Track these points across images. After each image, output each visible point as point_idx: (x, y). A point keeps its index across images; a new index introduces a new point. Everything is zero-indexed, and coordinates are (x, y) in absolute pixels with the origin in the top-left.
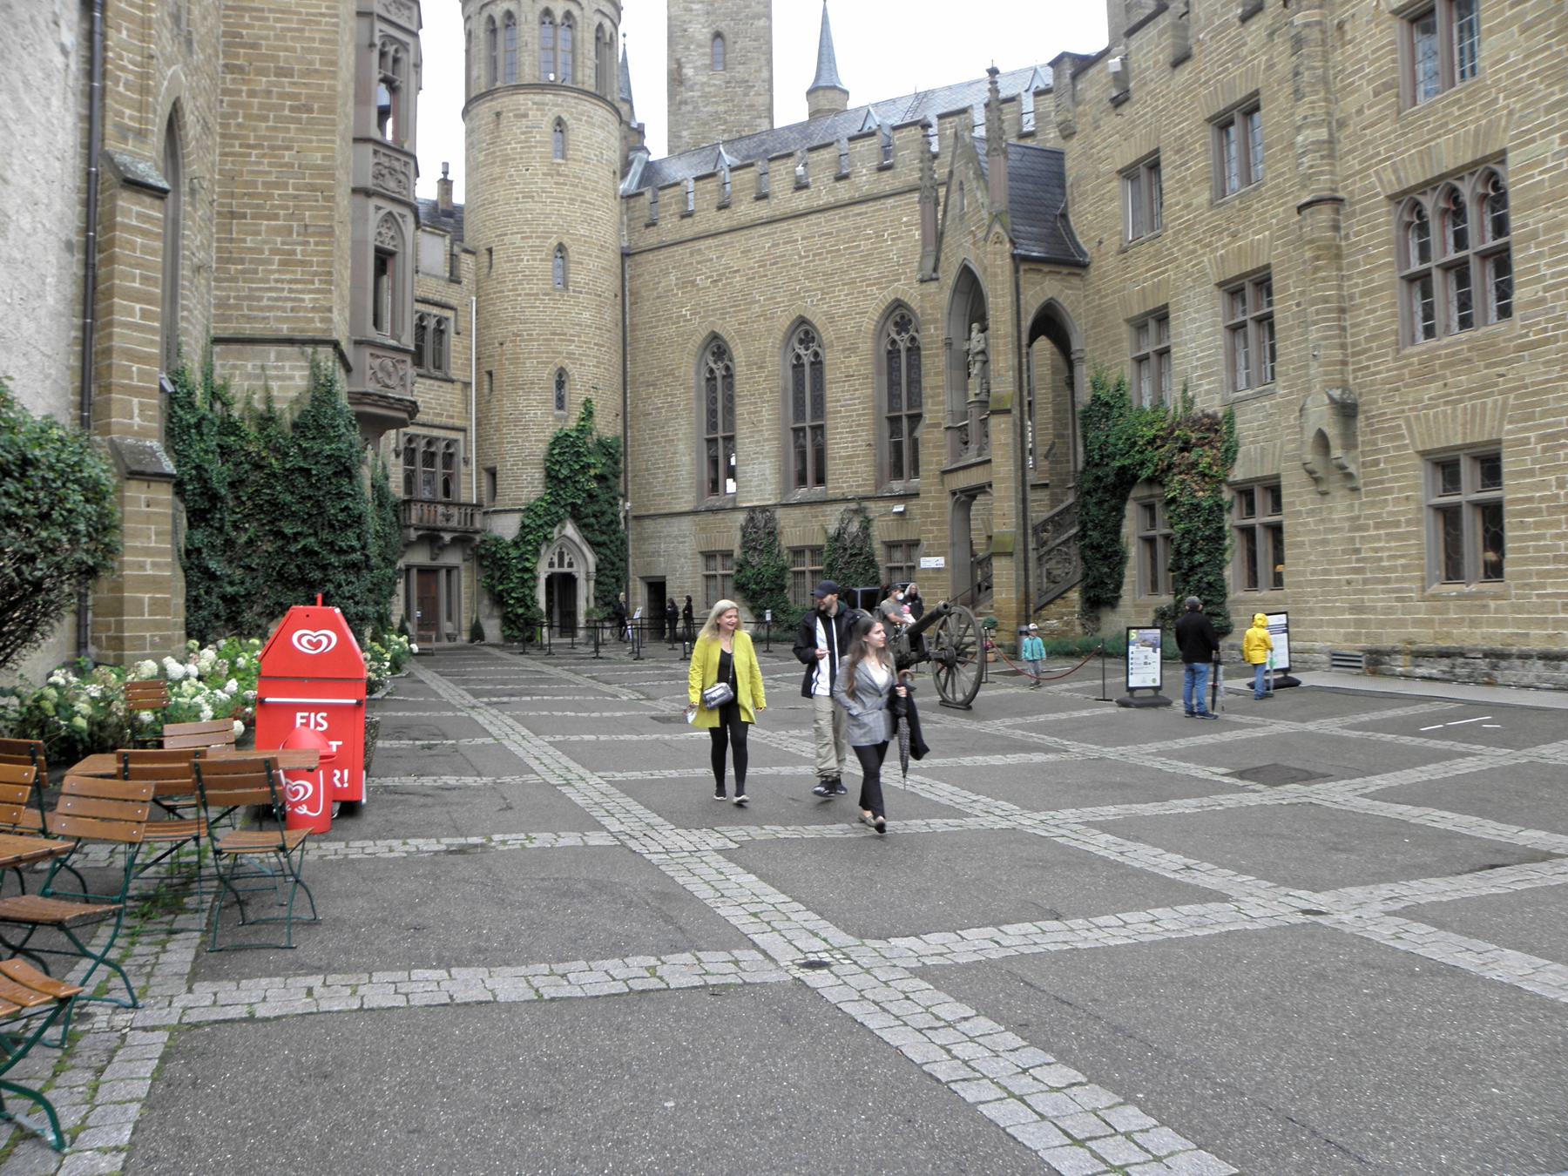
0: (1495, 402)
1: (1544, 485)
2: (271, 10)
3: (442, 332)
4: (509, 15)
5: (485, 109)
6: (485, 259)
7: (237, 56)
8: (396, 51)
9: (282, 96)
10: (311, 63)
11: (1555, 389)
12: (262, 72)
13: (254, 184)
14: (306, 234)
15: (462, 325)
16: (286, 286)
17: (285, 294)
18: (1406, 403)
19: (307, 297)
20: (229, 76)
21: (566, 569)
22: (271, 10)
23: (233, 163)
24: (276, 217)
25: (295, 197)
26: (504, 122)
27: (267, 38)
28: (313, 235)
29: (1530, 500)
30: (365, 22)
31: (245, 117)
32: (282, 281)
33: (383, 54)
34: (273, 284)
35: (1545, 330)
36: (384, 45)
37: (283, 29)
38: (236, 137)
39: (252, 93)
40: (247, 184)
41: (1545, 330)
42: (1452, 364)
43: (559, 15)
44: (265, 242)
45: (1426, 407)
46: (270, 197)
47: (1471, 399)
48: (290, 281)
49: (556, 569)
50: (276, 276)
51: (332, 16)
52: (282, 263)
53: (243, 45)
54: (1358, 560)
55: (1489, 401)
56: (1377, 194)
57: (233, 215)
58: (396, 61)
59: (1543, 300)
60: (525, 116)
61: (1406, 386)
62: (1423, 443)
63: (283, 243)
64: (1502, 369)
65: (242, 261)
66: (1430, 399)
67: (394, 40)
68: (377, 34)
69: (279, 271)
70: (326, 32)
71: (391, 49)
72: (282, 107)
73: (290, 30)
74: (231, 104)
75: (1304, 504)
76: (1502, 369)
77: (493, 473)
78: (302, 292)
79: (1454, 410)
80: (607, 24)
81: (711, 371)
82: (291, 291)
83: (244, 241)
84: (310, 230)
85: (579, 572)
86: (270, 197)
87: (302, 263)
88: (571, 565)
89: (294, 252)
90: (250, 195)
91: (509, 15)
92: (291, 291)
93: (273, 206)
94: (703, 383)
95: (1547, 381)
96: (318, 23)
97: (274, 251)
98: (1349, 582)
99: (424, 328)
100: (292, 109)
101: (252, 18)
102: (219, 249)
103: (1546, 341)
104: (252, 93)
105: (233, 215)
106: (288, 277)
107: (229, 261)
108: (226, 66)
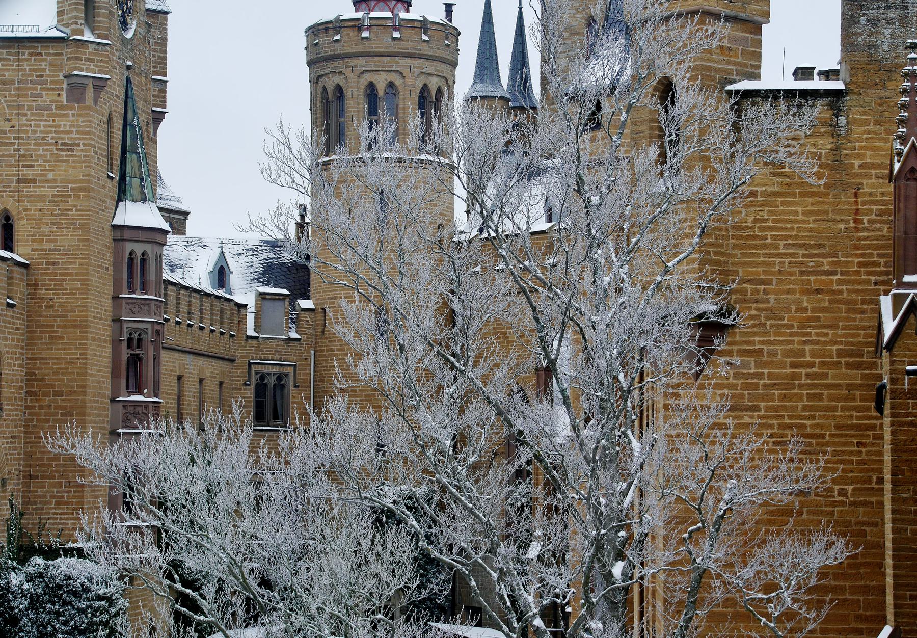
2: (50, 358)
3: (283, 386)
6: (320, 317)
7: (33, 386)
8: (140, 335)
9: (56, 408)
10: (72, 387)
12: (46, 395)
13: (42, 459)
14: (70, 487)
15: (301, 376)
16: (59, 516)
17: (58, 521)
19: (69, 522)
20: (29, 398)
22: (50, 358)
23: (31, 447)
24: (53, 477)
25: (64, 465)
27: (48, 374)
28: (74, 486)
30: (117, 325)
31: (38, 421)
32: (56, 514)
34: (52, 516)
37: (57, 369)
38: (32, 433)
39: (41, 407)
40: (38, 459)
44: (47, 492)
46: (50, 466)
48: (61, 514)
50: (54, 511)
51: (83, 359)
52: (57, 503)
53: (36, 380)
57: (30, 477)
63: (57, 492)
65: (35, 503)
67: (136, 330)
68: (125, 330)
69: (55, 508)
70: (80, 368)
71: (136, 336)
72: (57, 414)
73: (61, 369)
74: (30, 414)
78: (67, 519)
80: (434, 83)
82: (61, 519)
83: (37, 492)
84: (72, 484)
86: (50, 466)
87: (67, 503)
89: (63, 497)
90: (40, 466)
91: (339, 89)
92: (61, 519)
93: (52, 471)
96: (76, 364)
97: (52, 497)
99: (266, 385)
100: (62, 415)
101: (40, 364)
102: (23, 497)
104: (41, 407)
105: (30, 477)
106: (60, 511)
107: (28, 503)
108: (27, 392)
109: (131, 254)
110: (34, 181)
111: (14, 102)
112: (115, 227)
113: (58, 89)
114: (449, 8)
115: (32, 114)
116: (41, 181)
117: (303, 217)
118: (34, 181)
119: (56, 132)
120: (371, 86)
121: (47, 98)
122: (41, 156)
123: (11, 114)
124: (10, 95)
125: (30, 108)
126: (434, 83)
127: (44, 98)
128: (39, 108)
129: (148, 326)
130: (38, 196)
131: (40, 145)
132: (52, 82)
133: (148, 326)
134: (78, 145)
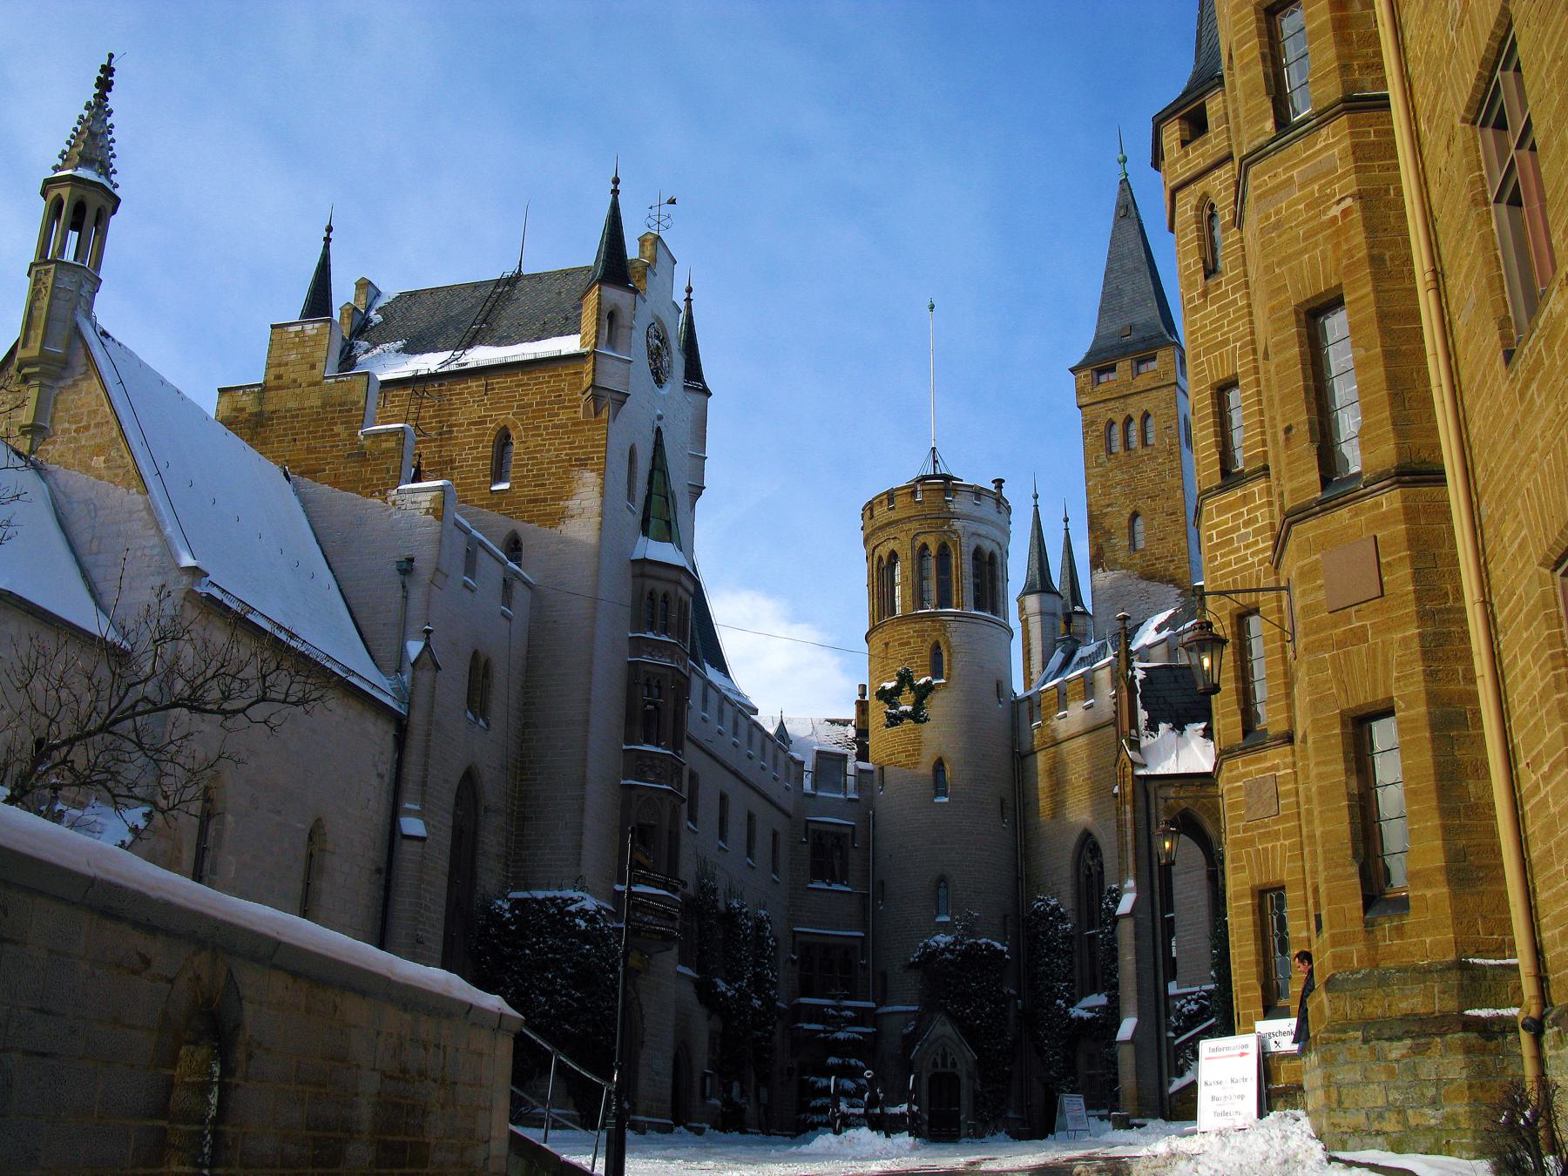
4: (893, 556)
5: (875, 639)
8: (659, 682)
21: (949, 1069)
26: (891, 650)
33: (649, 686)
36: (648, 680)
43: (933, 549)
49: (940, 1069)
58: (659, 688)
60: (908, 643)
71: (654, 683)
77: (884, 976)
81: (1089, 869)
85: (962, 1071)
88: (954, 1065)
94: (1082, 880)
109: (651, 593)
110: (545, 500)
111: (530, 424)
112: (633, 562)
113: (575, 407)
114: (999, 483)
115: (548, 434)
116: (552, 499)
117: (863, 695)
118: (545, 500)
119: (570, 449)
120: (925, 547)
121: (563, 416)
122: (553, 474)
123: (526, 436)
124: (527, 418)
125: (546, 428)
126: (988, 546)
127: (560, 417)
128: (554, 427)
129: (669, 672)
130: (550, 514)
131: (552, 462)
132: (570, 401)
133: (669, 672)
134: (593, 459)
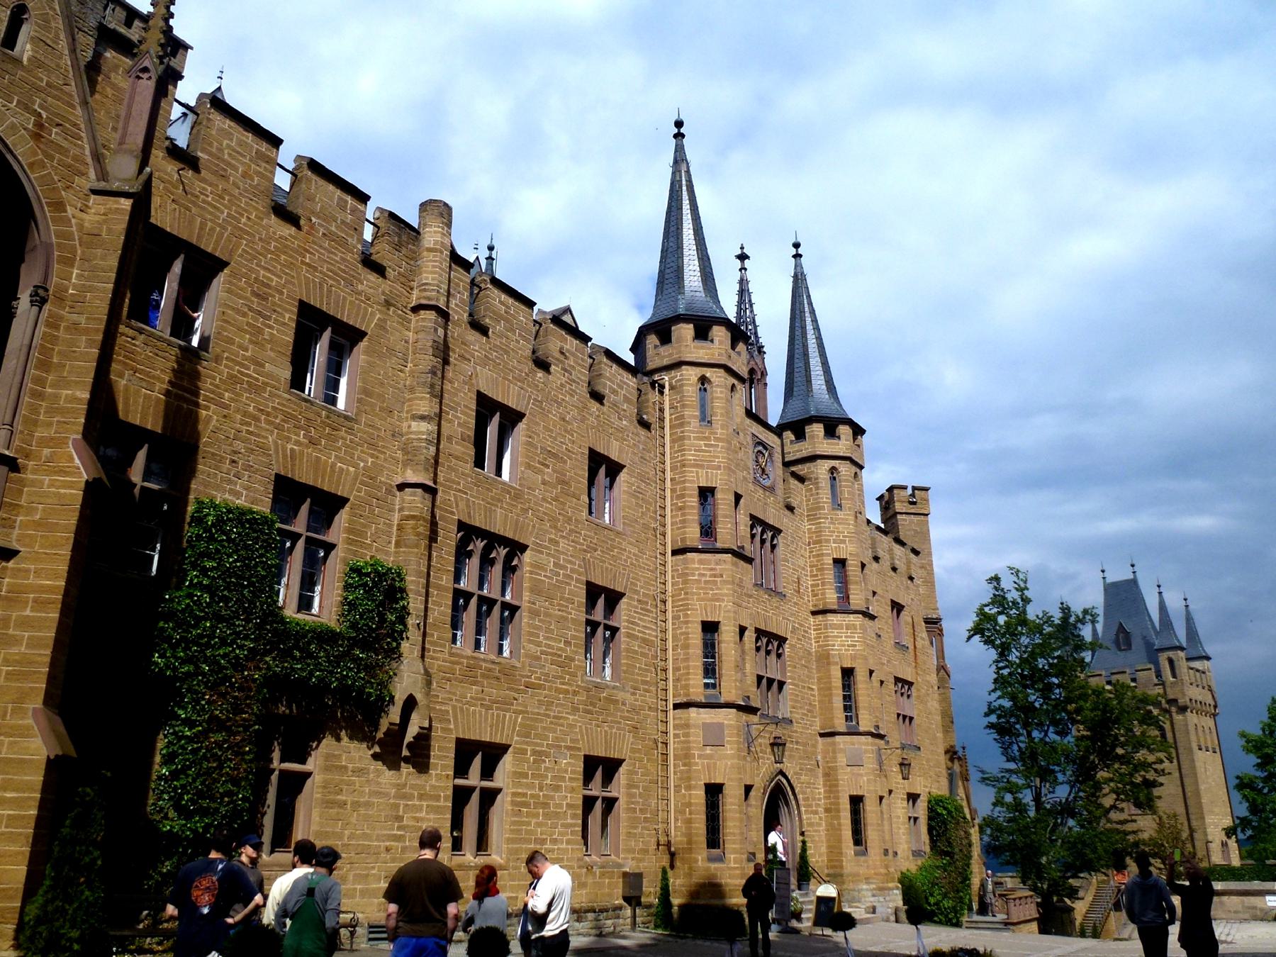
0: (511, 717)
1: (532, 786)
11: (541, 721)
18: (454, 694)
29: (525, 795)
35: (540, 679)
41: (540, 679)
42: (488, 677)
45: (467, 703)
47: (497, 709)
54: (399, 828)
55: (508, 714)
56: (452, 513)
59: (538, 658)
61: (456, 679)
62: (464, 732)
64: (516, 695)
66: (471, 697)
75: (351, 760)
76: (516, 695)
79: (486, 713)
95: (538, 714)
98: (388, 850)
103: (540, 687)
